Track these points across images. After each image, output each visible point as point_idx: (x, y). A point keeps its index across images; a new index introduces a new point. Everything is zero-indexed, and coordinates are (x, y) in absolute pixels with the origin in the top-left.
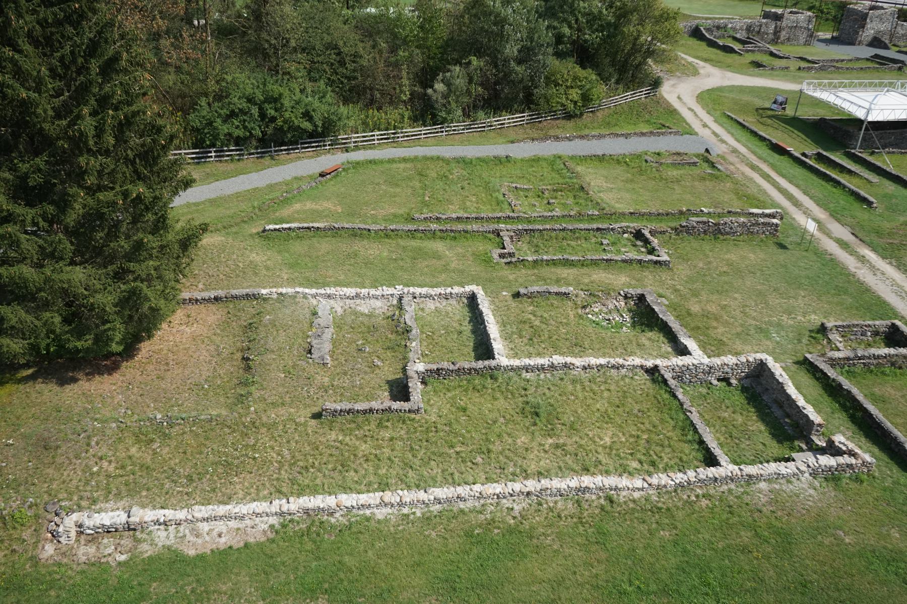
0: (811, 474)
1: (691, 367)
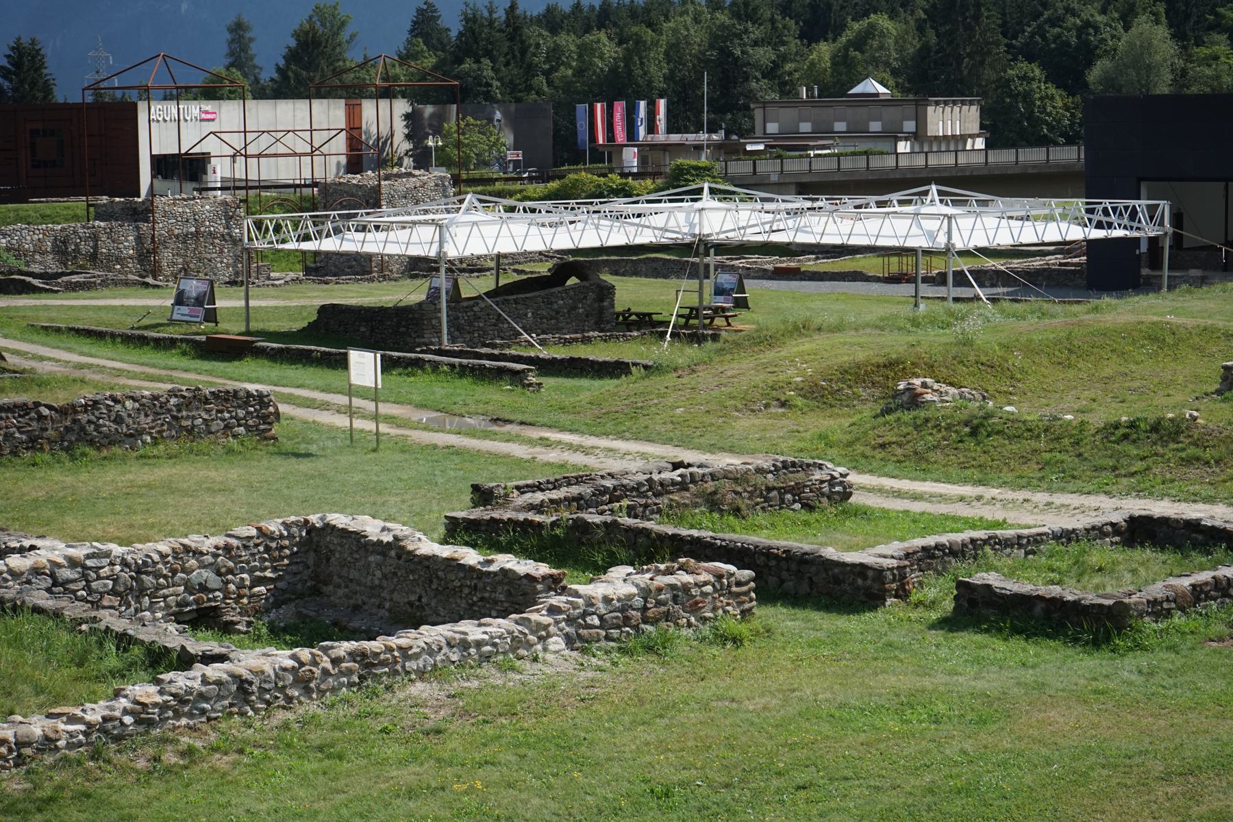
0: (569, 641)
1: (66, 573)
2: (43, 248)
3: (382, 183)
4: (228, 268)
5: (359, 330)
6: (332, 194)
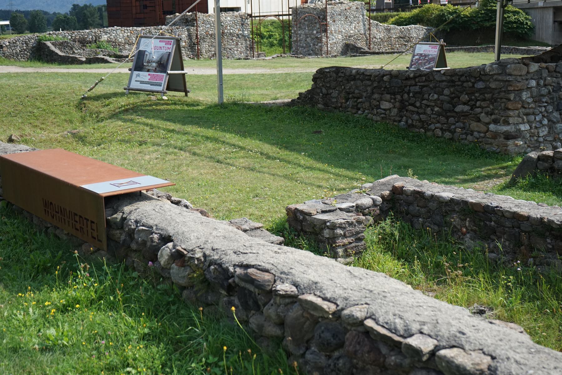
2: (130, 41)
3: (328, 6)
4: (241, 54)
5: (378, 107)
6: (299, 13)
